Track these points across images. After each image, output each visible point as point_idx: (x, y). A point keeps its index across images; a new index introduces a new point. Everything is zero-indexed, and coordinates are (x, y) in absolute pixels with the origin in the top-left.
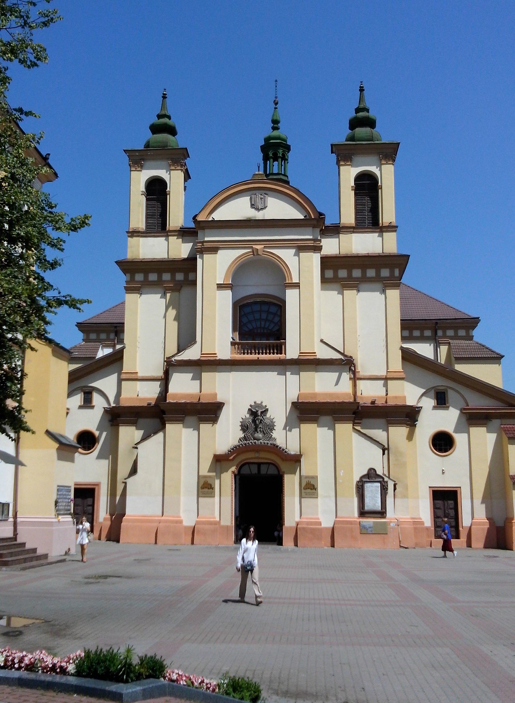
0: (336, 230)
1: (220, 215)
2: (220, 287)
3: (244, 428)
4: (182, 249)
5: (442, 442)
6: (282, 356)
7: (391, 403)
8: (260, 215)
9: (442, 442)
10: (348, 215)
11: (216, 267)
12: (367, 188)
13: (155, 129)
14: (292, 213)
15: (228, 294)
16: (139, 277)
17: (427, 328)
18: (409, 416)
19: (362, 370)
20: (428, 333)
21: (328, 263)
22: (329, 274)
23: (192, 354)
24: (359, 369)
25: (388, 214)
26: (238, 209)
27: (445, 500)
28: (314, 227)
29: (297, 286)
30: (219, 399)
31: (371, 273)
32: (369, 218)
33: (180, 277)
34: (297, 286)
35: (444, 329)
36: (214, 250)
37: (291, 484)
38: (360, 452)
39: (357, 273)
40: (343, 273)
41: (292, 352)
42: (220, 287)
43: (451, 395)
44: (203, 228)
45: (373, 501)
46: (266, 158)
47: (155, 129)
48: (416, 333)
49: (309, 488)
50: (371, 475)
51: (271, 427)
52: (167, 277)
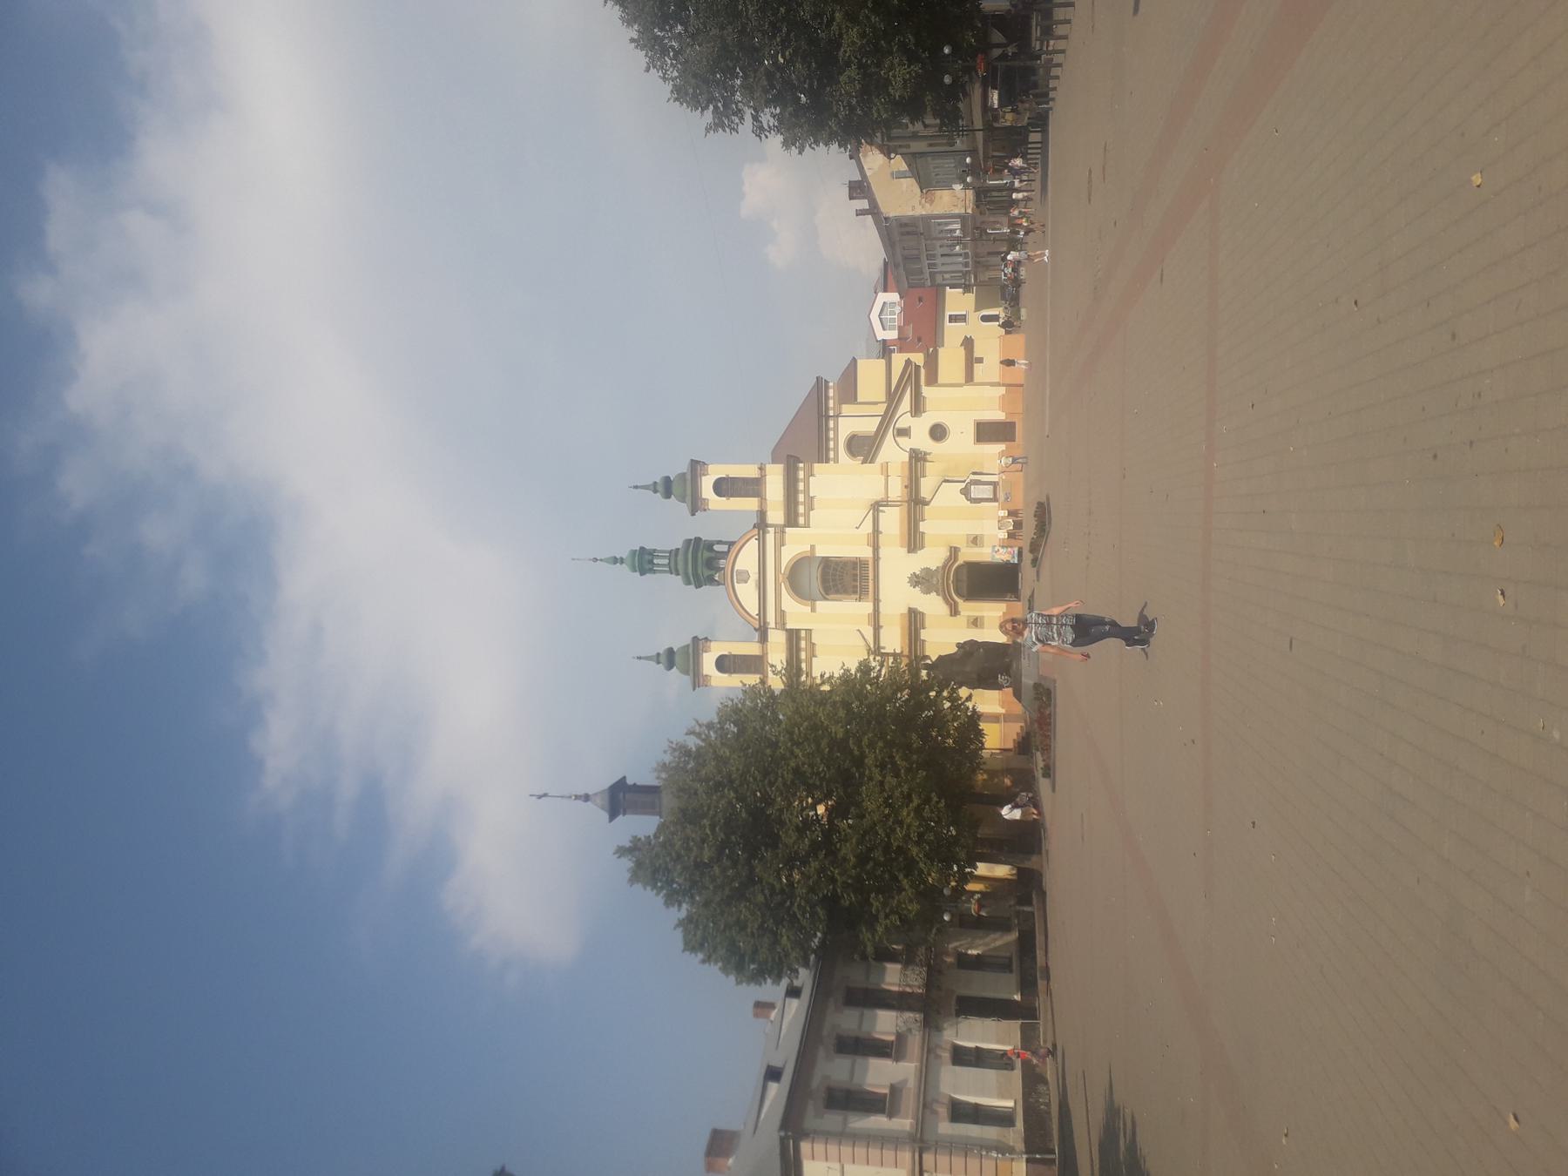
0: (762, 514)
1: (753, 609)
2: (813, 610)
3: (927, 591)
4: (777, 639)
5: (938, 432)
7: (907, 473)
10: (751, 504)
12: (724, 487)
13: (670, 665)
19: (878, 495)
21: (791, 520)
22: (801, 520)
23: (869, 632)
24: (879, 498)
25: (750, 471)
26: (747, 594)
27: (987, 432)
28: (764, 533)
29: (813, 547)
30: (905, 611)
31: (801, 486)
32: (752, 487)
34: (813, 547)
35: (827, 409)
37: (969, 554)
38: (945, 500)
39: (801, 498)
40: (801, 509)
42: (813, 610)
43: (901, 424)
45: (986, 492)
46: (652, 571)
47: (670, 665)
48: (831, 434)
49: (975, 541)
50: (965, 492)
51: (927, 570)
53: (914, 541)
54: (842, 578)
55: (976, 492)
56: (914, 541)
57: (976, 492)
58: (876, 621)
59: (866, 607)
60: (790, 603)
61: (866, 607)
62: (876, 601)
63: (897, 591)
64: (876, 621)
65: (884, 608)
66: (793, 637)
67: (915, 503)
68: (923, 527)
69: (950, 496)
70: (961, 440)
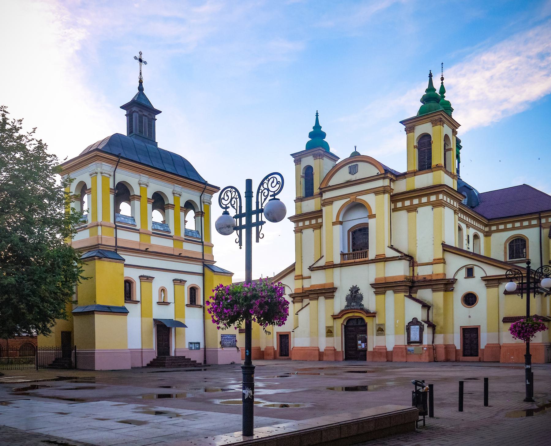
2: (334, 224)
6: (366, 259)
8: (353, 177)
9: (470, 299)
11: (331, 212)
14: (374, 171)
15: (338, 227)
16: (301, 224)
17: (533, 219)
18: (448, 285)
20: (534, 222)
23: (322, 263)
33: (320, 220)
36: (329, 202)
41: (372, 255)
42: (334, 224)
44: (325, 192)
48: (526, 223)
50: (414, 322)
52: (314, 222)
53: (381, 287)
54: (359, 239)
55: (415, 330)
56: (381, 287)
57: (415, 330)
58: (331, 266)
59: (337, 260)
60: (338, 205)
61: (337, 260)
62: (341, 265)
63: (346, 279)
64: (331, 266)
65: (337, 271)
66: (318, 214)
67: (410, 286)
68: (390, 293)
69: (415, 311)
70: (462, 316)
